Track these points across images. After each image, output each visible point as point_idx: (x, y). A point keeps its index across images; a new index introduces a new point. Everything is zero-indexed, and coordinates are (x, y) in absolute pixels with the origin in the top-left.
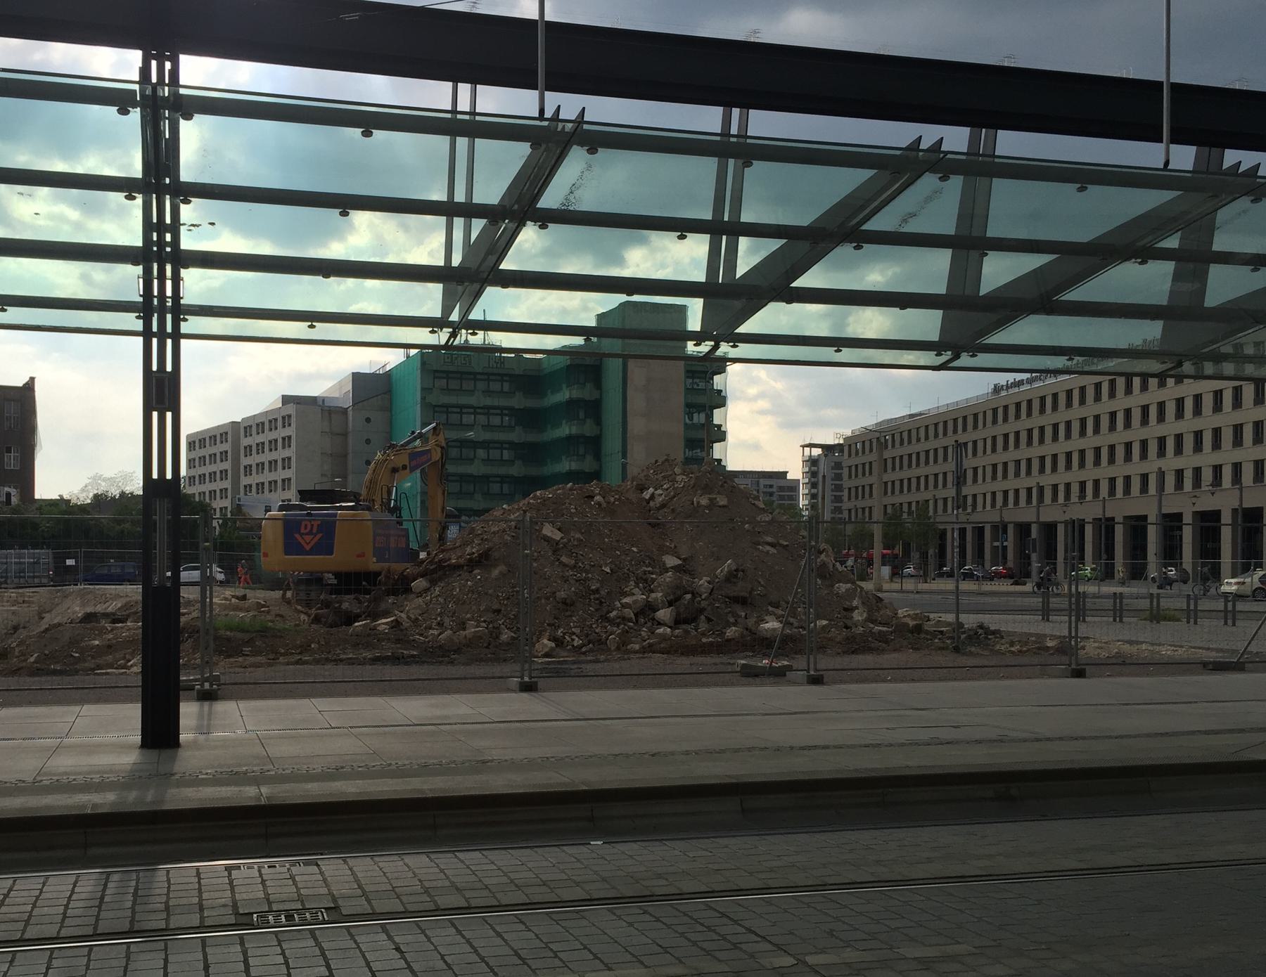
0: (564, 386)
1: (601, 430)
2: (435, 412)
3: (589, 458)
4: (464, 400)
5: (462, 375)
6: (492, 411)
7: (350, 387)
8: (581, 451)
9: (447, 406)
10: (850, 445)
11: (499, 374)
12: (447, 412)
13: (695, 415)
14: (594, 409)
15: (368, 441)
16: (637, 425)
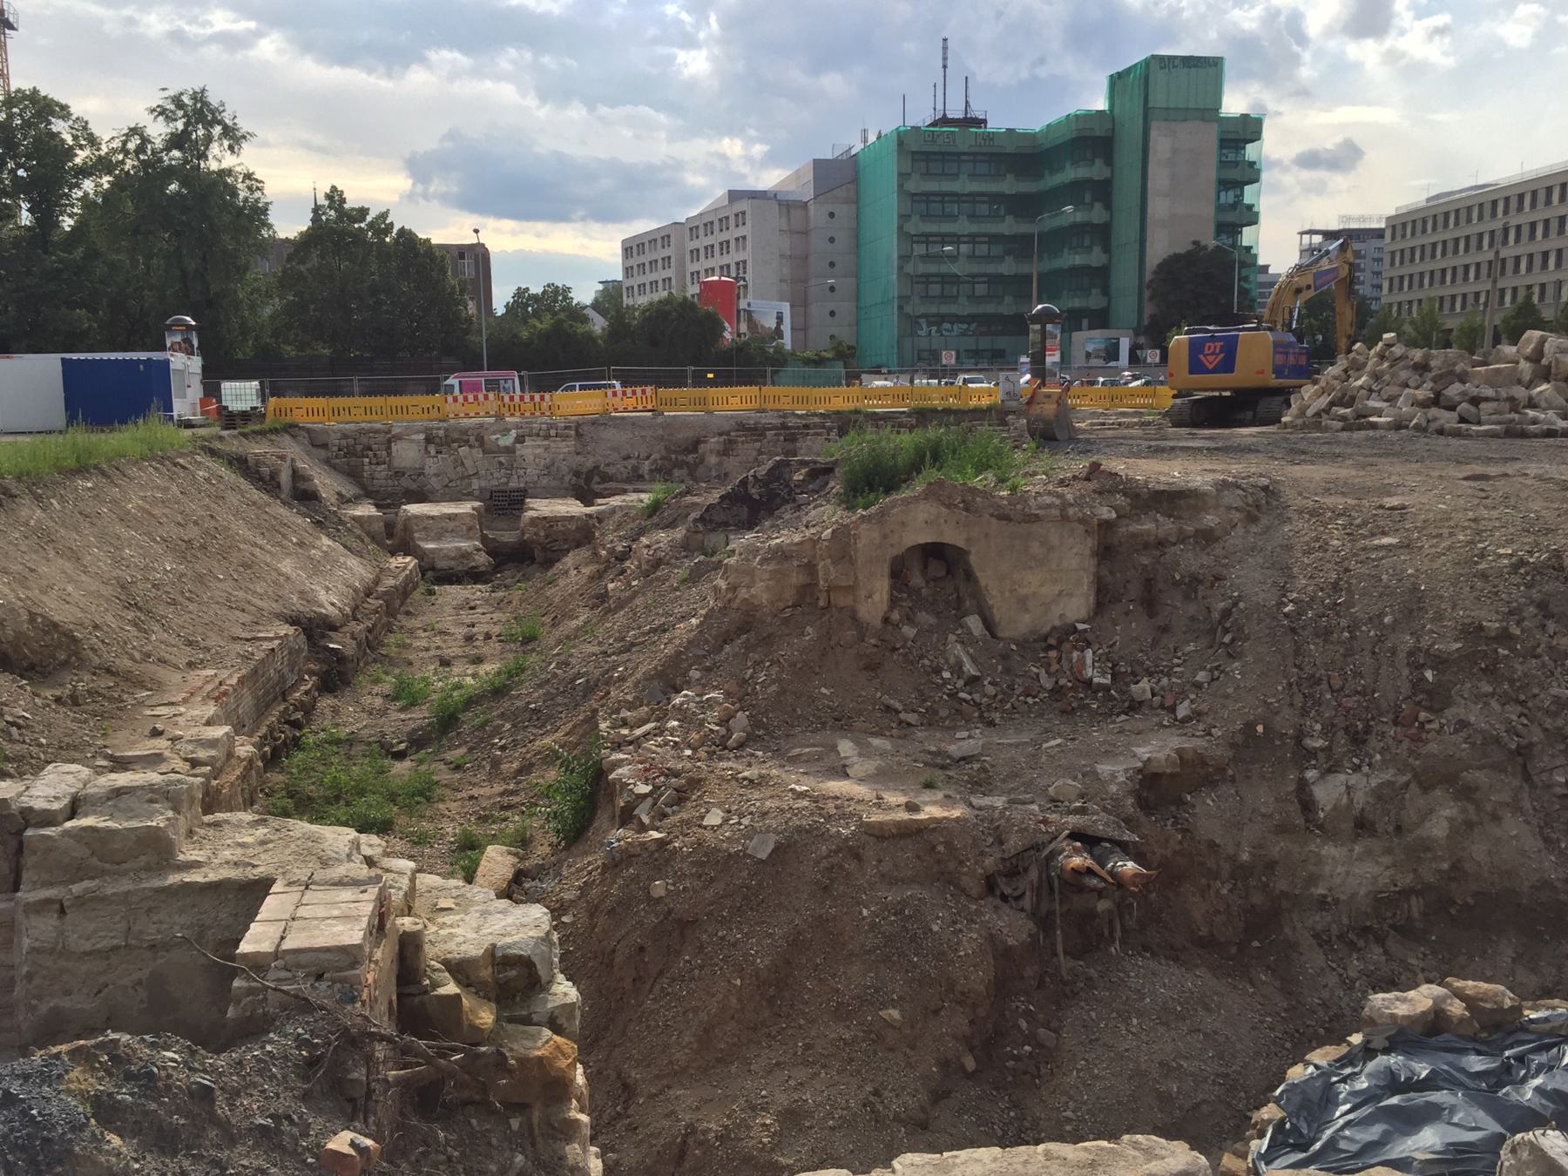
0: (1068, 165)
1: (1111, 216)
3: (1097, 250)
4: (947, 186)
5: (943, 156)
6: (977, 199)
7: (811, 176)
8: (1087, 242)
9: (927, 195)
11: (985, 154)
12: (927, 202)
13: (1223, 194)
14: (1103, 191)
16: (1158, 208)
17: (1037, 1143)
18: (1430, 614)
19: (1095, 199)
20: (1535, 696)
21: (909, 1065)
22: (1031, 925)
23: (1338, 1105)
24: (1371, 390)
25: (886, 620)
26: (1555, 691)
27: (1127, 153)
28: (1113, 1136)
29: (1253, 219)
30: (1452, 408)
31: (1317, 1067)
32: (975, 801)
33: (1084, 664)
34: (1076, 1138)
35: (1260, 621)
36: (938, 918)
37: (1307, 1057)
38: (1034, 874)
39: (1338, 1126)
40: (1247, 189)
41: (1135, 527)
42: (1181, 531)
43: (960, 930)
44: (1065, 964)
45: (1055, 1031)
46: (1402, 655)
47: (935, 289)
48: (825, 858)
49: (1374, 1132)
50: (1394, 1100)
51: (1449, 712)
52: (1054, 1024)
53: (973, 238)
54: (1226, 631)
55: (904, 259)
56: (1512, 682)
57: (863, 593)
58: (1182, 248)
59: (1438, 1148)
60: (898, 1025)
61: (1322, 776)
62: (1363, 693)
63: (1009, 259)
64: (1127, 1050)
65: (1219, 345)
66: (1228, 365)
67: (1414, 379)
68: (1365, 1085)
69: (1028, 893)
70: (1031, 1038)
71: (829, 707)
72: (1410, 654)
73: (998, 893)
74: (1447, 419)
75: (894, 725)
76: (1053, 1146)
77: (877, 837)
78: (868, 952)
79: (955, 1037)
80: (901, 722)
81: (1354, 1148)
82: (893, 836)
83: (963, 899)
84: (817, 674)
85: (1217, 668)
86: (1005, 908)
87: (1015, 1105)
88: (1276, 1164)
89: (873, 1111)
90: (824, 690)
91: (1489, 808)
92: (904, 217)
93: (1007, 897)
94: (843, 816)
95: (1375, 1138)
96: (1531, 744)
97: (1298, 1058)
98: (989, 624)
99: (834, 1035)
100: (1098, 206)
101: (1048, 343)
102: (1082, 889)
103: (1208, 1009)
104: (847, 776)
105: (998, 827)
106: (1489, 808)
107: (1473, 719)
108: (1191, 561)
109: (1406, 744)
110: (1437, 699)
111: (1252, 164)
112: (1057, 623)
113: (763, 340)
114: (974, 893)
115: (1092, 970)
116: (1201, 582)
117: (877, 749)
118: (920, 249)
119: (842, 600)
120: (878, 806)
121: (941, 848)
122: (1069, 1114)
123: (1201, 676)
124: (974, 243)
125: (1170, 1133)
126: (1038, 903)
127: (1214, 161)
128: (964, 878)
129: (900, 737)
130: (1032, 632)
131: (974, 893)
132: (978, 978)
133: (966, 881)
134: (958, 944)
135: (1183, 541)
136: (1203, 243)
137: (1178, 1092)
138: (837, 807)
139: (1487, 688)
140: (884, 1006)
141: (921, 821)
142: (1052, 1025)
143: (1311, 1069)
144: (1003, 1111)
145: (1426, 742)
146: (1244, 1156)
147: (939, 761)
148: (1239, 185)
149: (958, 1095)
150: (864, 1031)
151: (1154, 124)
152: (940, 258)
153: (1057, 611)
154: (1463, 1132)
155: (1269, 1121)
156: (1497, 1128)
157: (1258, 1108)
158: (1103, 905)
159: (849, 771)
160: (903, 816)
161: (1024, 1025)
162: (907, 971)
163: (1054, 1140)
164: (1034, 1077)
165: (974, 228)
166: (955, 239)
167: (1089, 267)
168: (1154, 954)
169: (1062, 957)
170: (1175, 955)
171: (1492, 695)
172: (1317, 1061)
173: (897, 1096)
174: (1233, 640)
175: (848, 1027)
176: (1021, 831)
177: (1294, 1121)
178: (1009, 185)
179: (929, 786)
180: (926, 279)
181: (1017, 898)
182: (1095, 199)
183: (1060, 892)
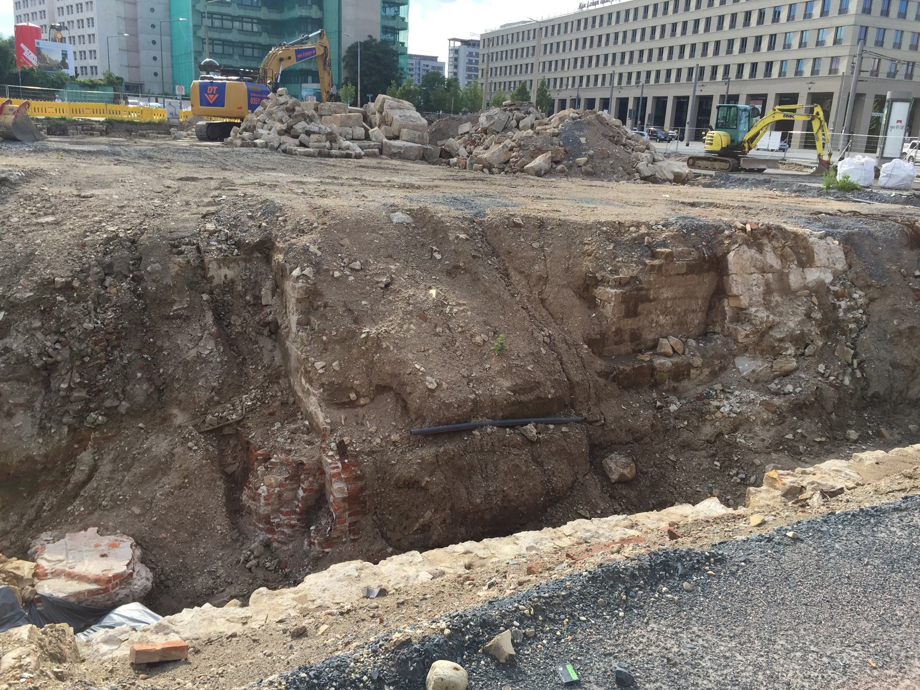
13: (388, 9)
15: (152, 10)
16: (348, 13)
19: (313, 3)
26: (85, 325)
40: (402, 8)
53: (240, 19)
55: (197, 27)
58: (363, 38)
100: (315, 7)
113: (51, 69)
124: (242, 22)
136: (374, 37)
139: (37, 324)
171: (39, 328)
182: (313, 3)
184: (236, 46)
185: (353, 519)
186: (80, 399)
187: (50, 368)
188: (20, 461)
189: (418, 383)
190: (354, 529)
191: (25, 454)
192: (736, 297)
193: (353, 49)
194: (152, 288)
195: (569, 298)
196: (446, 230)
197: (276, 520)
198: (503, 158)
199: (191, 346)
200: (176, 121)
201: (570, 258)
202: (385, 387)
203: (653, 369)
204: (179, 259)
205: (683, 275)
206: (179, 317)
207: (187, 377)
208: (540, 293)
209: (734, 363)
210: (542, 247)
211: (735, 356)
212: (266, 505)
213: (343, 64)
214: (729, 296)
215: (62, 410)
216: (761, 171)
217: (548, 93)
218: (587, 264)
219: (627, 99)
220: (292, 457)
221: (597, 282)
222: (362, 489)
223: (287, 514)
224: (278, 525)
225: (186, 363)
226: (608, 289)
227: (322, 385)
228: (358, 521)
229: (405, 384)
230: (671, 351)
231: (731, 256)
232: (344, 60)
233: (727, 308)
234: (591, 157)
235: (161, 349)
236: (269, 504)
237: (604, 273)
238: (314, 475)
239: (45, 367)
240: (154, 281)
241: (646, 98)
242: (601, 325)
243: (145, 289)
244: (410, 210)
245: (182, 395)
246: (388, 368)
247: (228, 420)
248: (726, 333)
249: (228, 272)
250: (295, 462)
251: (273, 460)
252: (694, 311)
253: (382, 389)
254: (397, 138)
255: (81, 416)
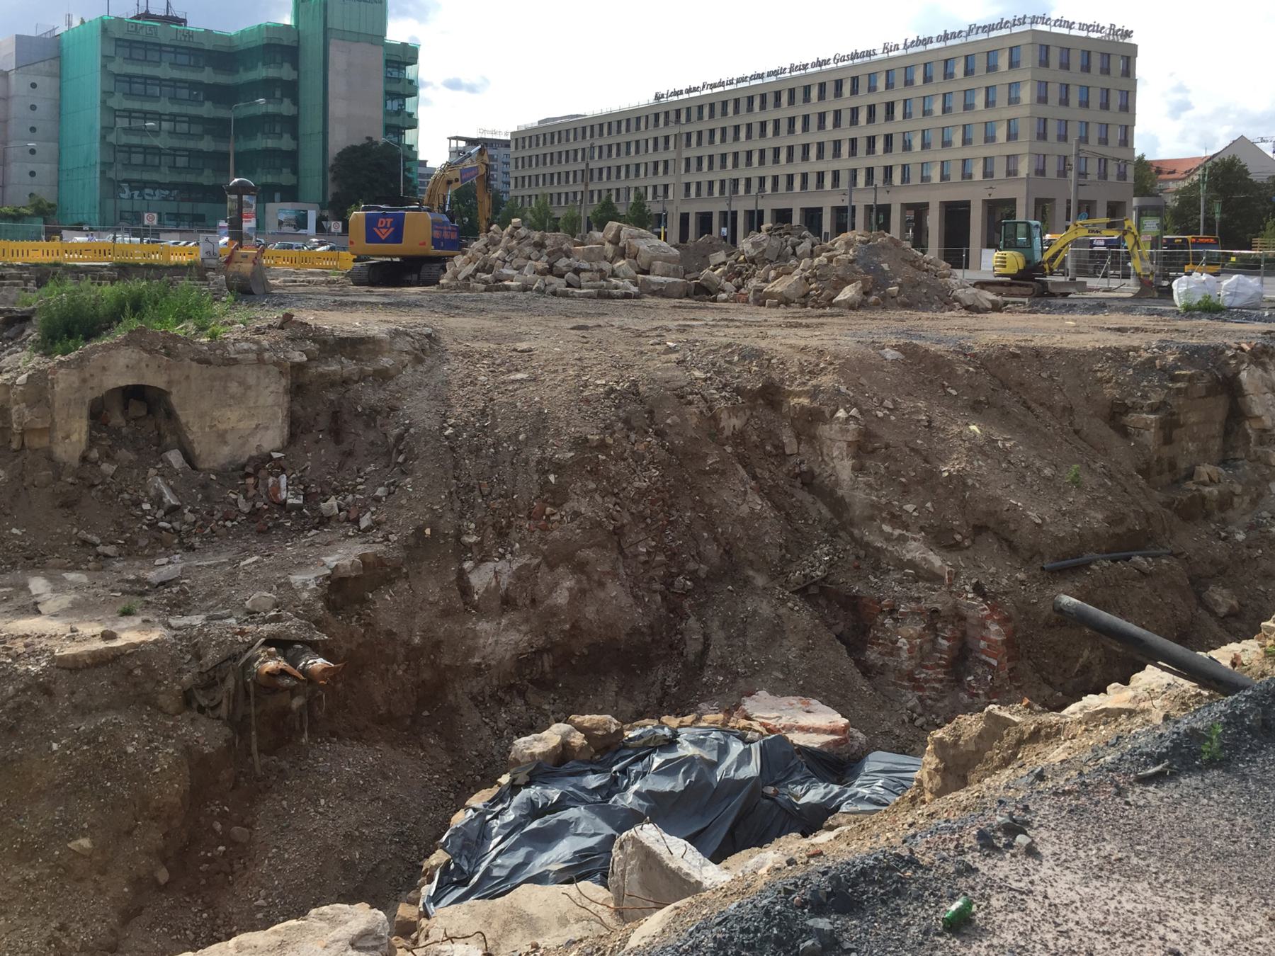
2: (116, 81)
3: (286, 137)
4: (148, 71)
8: (278, 130)
10: (517, 140)
13: (389, 102)
14: (291, 89)
16: (337, 108)
17: (229, 937)
18: (552, 431)
19: (283, 96)
20: (624, 489)
21: (100, 891)
22: (227, 731)
23: (491, 839)
24: (505, 261)
25: (84, 459)
26: (637, 484)
27: (311, 59)
28: (301, 913)
29: (414, 125)
30: (561, 276)
31: (475, 810)
32: (174, 622)
33: (279, 488)
34: (267, 924)
35: (426, 443)
36: (133, 739)
37: (467, 803)
38: (230, 683)
39: (492, 857)
41: (324, 369)
42: (362, 370)
43: (157, 748)
44: (259, 761)
45: (248, 826)
46: (533, 464)
47: (137, 159)
48: (12, 698)
49: (519, 856)
50: (535, 825)
51: (567, 506)
52: (248, 820)
53: (173, 118)
54: (400, 452)
55: (106, 130)
56: (608, 479)
57: (60, 434)
58: (358, 142)
59: (569, 857)
60: (87, 854)
61: (476, 567)
62: (505, 496)
63: (207, 138)
64: (315, 830)
65: (389, 220)
66: (397, 237)
67: (535, 254)
68: (512, 817)
69: (225, 701)
70: (227, 839)
71: (20, 546)
72: (539, 462)
73: (195, 706)
74: (559, 284)
75: (91, 558)
76: (244, 938)
77: (70, 670)
78: (58, 786)
79: (148, 854)
80: (98, 555)
81: (504, 873)
82: (88, 667)
83: (160, 718)
84: (6, 515)
85: (393, 484)
86: (203, 719)
87: (208, 906)
88: (444, 902)
89: (57, 947)
90: (15, 531)
91: (596, 578)
92: (107, 94)
93: (204, 708)
94: (33, 654)
95: (521, 860)
96: (623, 526)
97: (460, 805)
98: (189, 458)
99: (16, 878)
100: (287, 101)
101: (245, 211)
102: (275, 690)
103: (386, 778)
104: (39, 613)
105: (196, 644)
106: (596, 578)
107: (583, 510)
108: (371, 396)
109: (537, 534)
110: (558, 496)
111: (411, 82)
112: (254, 453)
114: (171, 709)
115: (284, 762)
116: (379, 413)
117: (72, 583)
118: (122, 123)
119: (37, 442)
120: (73, 639)
121: (138, 672)
122: (261, 902)
123: (380, 491)
125: (351, 899)
126: (234, 709)
127: (382, 74)
128: (160, 696)
129: (96, 570)
130: (230, 463)
131: (171, 709)
132: (173, 791)
133: (164, 700)
134: (153, 761)
135: (364, 380)
136: (374, 140)
137: (361, 858)
138: (26, 646)
139: (592, 486)
140: (74, 837)
141: (118, 648)
142: (245, 822)
143: (471, 812)
144: (195, 914)
145: (551, 531)
146: (415, 902)
147: (137, 588)
148: (402, 97)
149: (151, 909)
150: (50, 867)
151: (332, 41)
152: (143, 131)
153: (254, 442)
154: (585, 838)
155: (437, 866)
156: (608, 830)
157: (427, 857)
158: (297, 703)
159: (40, 607)
160: (100, 645)
161: (218, 826)
162: (99, 798)
163: (245, 931)
164: (227, 875)
165: (175, 109)
166: (158, 117)
167: (280, 150)
168: (340, 738)
169: (256, 757)
170: (359, 735)
171: (596, 490)
172: (475, 805)
173: (85, 925)
174: (405, 460)
175: (33, 867)
176: (218, 644)
177: (457, 861)
178: (207, 76)
179: (127, 613)
180: (129, 149)
181: (213, 709)
182: (283, 96)
183: (255, 696)
184: (164, 154)
185: (1012, 664)
186: (662, 564)
187: (618, 532)
188: (627, 634)
189: (1022, 519)
190: (1014, 675)
191: (630, 626)
192: (1259, 418)
193: (350, 154)
194: (679, 442)
195: (1100, 429)
196: (950, 364)
197: (923, 675)
198: (801, 291)
199: (740, 502)
200: (213, 262)
201: (1085, 386)
202: (981, 527)
203: (1203, 498)
204: (693, 409)
205: (1203, 397)
206: (715, 471)
207: (749, 535)
208: (1071, 424)
209: (1269, 489)
210: (1050, 376)
211: (1268, 481)
212: (911, 658)
213: (330, 176)
214: (1251, 418)
215: (647, 576)
216: (1065, 295)
217: (647, 209)
218: (1110, 392)
219: (711, 214)
220: (924, 605)
221: (1127, 410)
222: (1015, 631)
223: (932, 668)
224: (926, 681)
225: (742, 521)
226: (1144, 415)
227: (922, 529)
228: (1015, 668)
229: (1003, 522)
230: (1207, 478)
231: (1244, 375)
232: (332, 170)
233: (1250, 431)
234: (900, 285)
235: (711, 507)
236: (912, 658)
237: (1134, 400)
238: (953, 623)
239: (615, 532)
240: (678, 434)
241: (762, 211)
242: (1143, 455)
243: (672, 443)
244: (896, 346)
245: (751, 556)
246: (982, 506)
247: (813, 577)
248: (1253, 457)
249: (736, 422)
250: (928, 610)
251: (901, 610)
252: (1214, 437)
253: (979, 529)
254: (647, 272)
255: (668, 580)
